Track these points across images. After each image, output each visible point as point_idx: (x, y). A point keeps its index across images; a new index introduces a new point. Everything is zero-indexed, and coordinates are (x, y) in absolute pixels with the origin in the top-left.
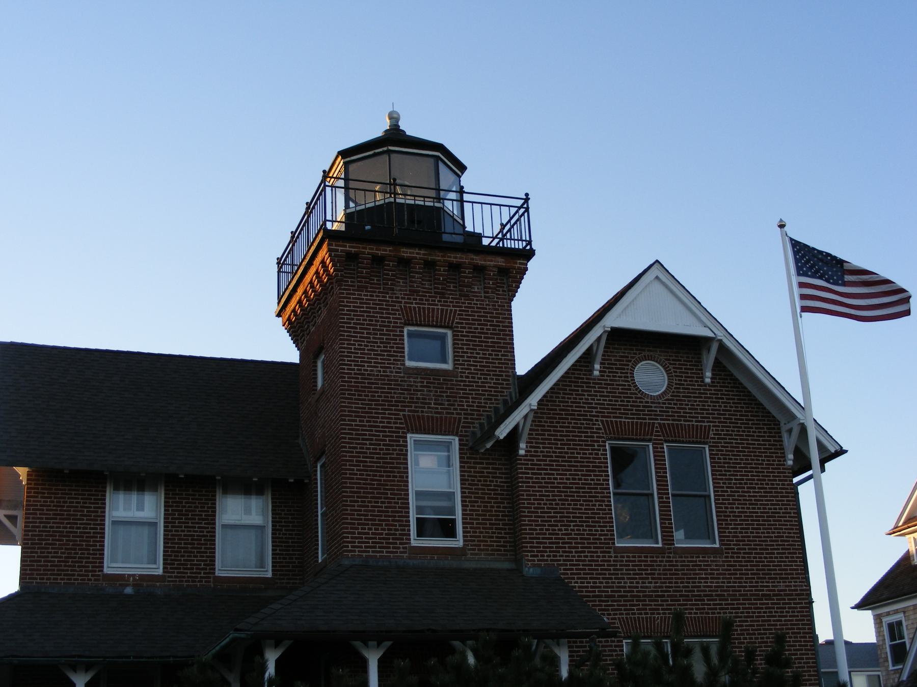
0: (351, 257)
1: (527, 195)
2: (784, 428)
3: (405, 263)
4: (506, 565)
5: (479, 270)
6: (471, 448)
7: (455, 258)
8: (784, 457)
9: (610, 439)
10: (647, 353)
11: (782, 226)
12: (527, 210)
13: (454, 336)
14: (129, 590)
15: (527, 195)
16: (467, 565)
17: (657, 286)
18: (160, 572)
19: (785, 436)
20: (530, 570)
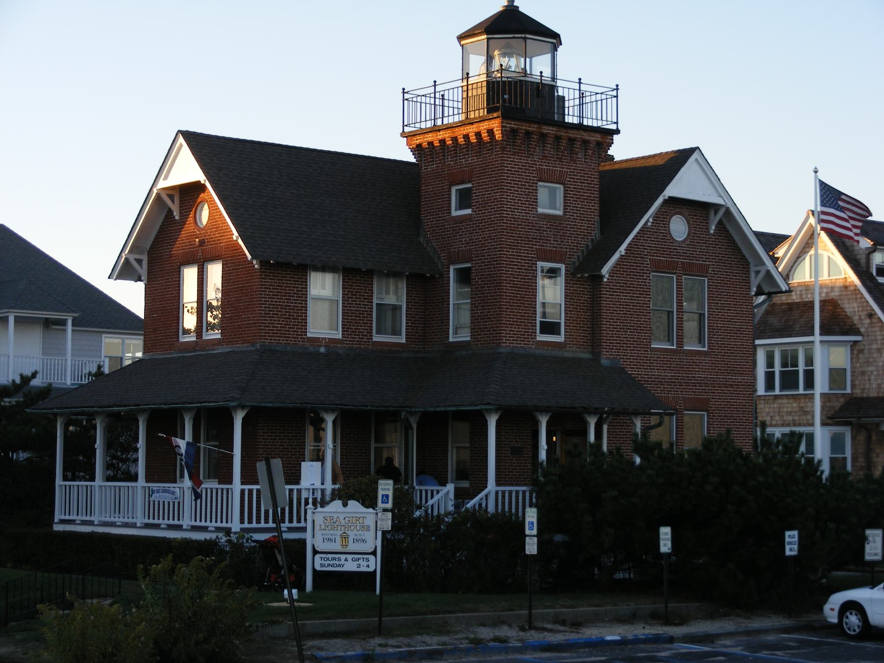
0: (514, 131)
1: (617, 86)
2: (753, 269)
3: (543, 136)
4: (587, 356)
5: (585, 142)
6: (572, 274)
7: (573, 134)
8: (749, 288)
9: (653, 271)
10: (677, 210)
11: (816, 172)
12: (617, 97)
13: (565, 190)
14: (322, 350)
15: (617, 86)
16: (567, 355)
17: (696, 167)
18: (340, 336)
19: (753, 275)
20: (604, 362)
